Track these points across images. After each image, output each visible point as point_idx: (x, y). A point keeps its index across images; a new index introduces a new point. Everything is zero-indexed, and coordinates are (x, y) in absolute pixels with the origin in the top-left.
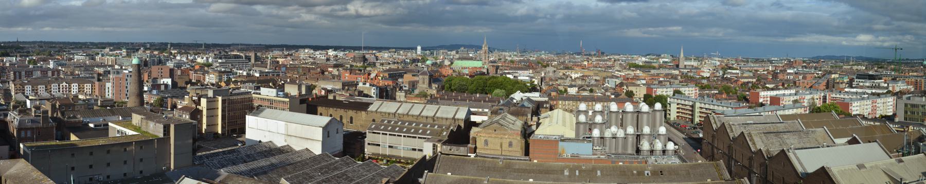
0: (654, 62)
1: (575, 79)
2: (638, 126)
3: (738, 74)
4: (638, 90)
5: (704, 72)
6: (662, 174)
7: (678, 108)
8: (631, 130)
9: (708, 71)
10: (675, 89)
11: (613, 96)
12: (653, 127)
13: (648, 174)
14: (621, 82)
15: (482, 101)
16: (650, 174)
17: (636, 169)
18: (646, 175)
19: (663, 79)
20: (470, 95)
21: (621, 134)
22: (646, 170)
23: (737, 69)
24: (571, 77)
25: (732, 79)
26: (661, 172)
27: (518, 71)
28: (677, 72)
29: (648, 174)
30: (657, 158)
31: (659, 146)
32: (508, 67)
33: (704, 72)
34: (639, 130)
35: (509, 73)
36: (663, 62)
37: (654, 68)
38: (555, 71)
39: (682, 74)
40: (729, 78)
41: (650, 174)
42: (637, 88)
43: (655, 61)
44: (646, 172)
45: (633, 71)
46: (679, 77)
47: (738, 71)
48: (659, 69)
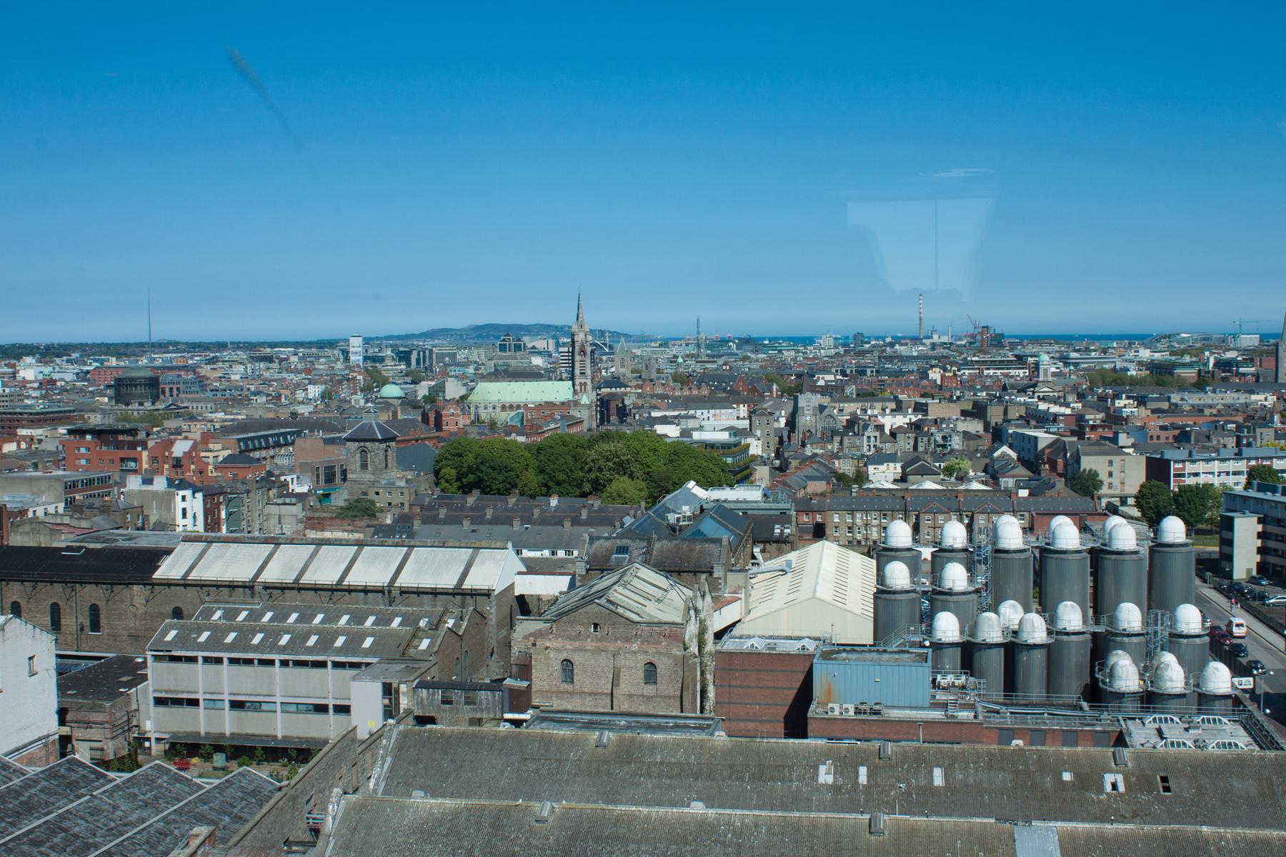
0: (1184, 365)
1: (893, 434)
2: (1099, 606)
4: (1115, 469)
6: (1167, 789)
8: (1072, 616)
10: (1253, 463)
11: (1024, 493)
13: (1114, 786)
14: (1057, 440)
15: (567, 524)
16: (1122, 788)
17: (1073, 765)
18: (1109, 788)
20: (526, 501)
21: (1036, 630)
22: (1111, 772)
24: (880, 428)
26: (1164, 779)
27: (699, 412)
29: (1114, 786)
30: (1164, 726)
31: (1174, 676)
32: (663, 397)
35: (665, 420)
36: (1218, 364)
38: (822, 408)
41: (1122, 788)
42: (1111, 463)
43: (1187, 359)
44: (1109, 778)
46: (1277, 418)
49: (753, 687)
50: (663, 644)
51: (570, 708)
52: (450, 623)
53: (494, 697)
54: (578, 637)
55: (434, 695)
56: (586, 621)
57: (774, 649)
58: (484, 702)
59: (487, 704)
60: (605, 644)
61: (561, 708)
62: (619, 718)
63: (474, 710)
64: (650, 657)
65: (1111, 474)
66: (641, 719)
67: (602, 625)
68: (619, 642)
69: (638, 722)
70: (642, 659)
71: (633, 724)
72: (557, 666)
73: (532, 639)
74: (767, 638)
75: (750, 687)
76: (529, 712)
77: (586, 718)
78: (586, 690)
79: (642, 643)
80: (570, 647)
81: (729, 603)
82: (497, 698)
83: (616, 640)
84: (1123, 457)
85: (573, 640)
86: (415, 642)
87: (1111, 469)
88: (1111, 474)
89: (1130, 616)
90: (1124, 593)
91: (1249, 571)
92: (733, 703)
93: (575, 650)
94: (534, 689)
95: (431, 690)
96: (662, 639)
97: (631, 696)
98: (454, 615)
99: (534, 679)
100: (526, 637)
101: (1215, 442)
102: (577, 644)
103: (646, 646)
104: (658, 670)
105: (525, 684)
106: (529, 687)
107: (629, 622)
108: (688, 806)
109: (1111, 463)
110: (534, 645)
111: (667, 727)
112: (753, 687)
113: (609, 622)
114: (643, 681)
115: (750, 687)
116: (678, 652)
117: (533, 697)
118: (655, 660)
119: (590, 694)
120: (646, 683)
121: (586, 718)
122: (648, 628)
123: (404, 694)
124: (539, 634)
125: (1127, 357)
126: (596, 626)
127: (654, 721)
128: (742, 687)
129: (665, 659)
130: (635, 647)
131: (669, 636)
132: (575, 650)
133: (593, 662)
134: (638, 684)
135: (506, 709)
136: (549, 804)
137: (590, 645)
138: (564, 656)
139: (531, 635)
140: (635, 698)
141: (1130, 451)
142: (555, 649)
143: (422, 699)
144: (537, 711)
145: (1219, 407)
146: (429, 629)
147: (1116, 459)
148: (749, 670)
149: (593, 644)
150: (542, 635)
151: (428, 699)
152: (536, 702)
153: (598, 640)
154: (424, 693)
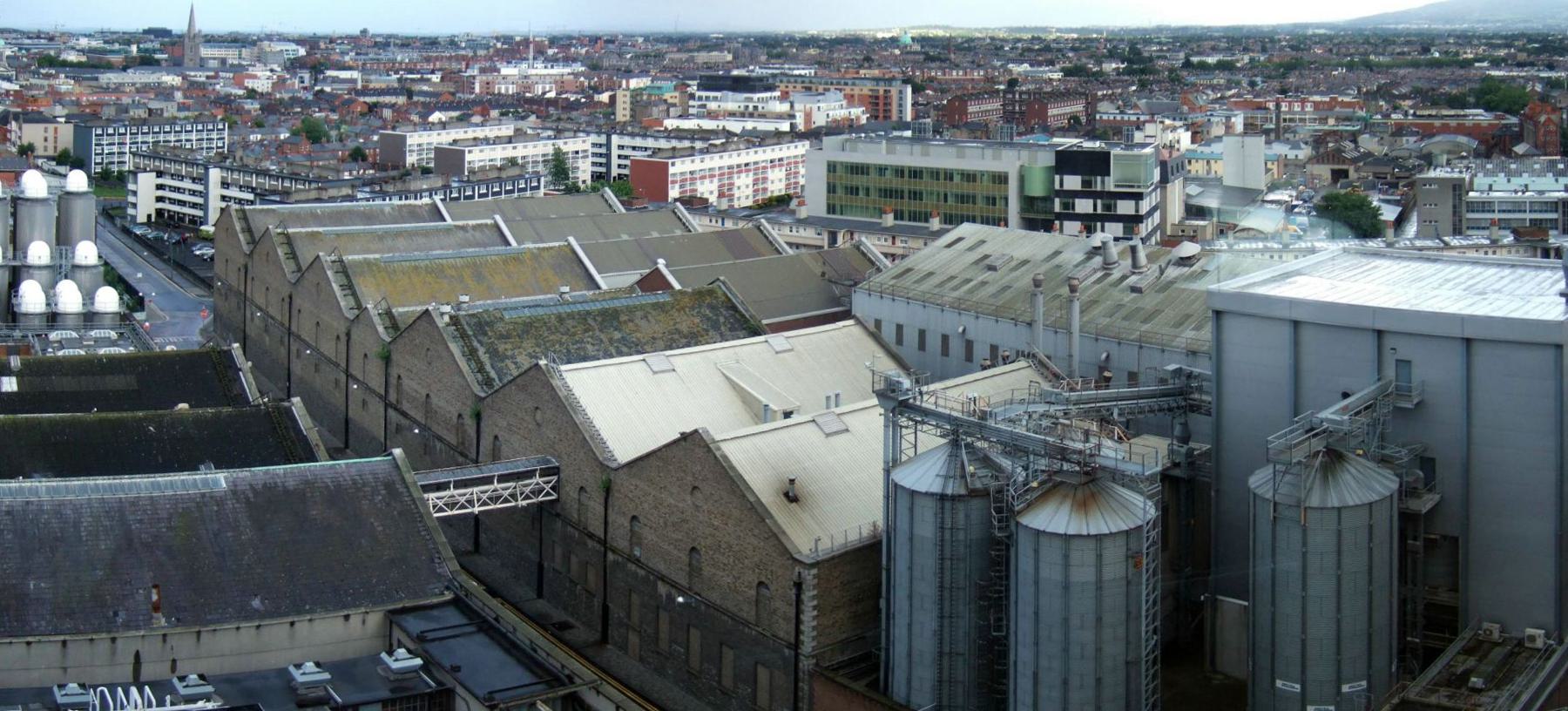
3: (354, 81)
5: (255, 77)
7: (160, 187)
9: (268, 73)
12: (63, 239)
19: (129, 101)
23: (350, 68)
25: (338, 96)
28: (175, 80)
33: (255, 77)
34: (19, 253)
37: (110, 67)
39: (191, 87)
40: (329, 94)
42: (46, 130)
43: (117, 46)
45: (48, 76)
47: (355, 74)
48: (125, 69)
65: (46, 140)
84: (56, 125)
87: (46, 135)
88: (46, 140)
89: (39, 252)
90: (36, 234)
91: (149, 216)
101: (132, 113)
109: (46, 130)
125: (70, 44)
141: (63, 120)
145: (138, 86)
147: (51, 127)
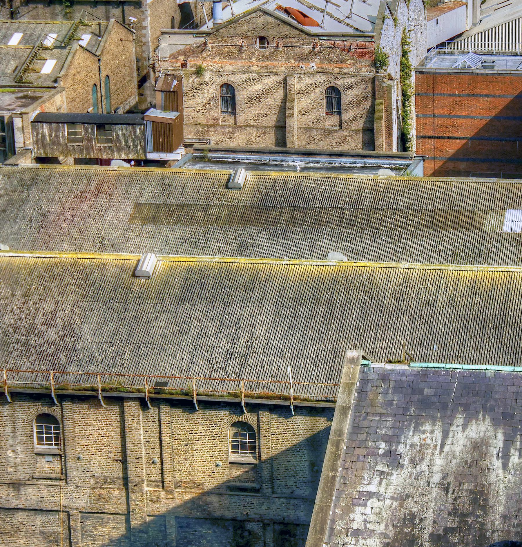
49: (465, 117)
50: (348, 62)
51: (232, 145)
52: (86, 39)
53: (135, 133)
54: (239, 54)
55: (57, 130)
56: (249, 34)
57: (492, 67)
58: (122, 139)
59: (126, 141)
60: (275, 63)
61: (220, 146)
62: (294, 157)
63: (110, 148)
64: (332, 80)
66: (322, 159)
67: (270, 40)
68: (292, 61)
69: (318, 162)
70: (323, 81)
71: (311, 165)
72: (216, 92)
73: (181, 58)
74: (485, 54)
75: (460, 117)
76: (179, 151)
77: (253, 158)
78: (252, 123)
79: (322, 60)
80: (231, 68)
81: (450, 9)
82: (138, 133)
83: (288, 58)
85: (234, 58)
86: (37, 64)
92: (438, 138)
93: (237, 72)
94: (186, 122)
95: (54, 125)
96: (348, 57)
97: (309, 129)
98: (90, 29)
99: (185, 110)
100: (173, 56)
102: (239, 63)
103: (327, 66)
104: (343, 96)
105: (171, 115)
106: (181, 117)
107: (304, 36)
108: (324, 257)
110: (184, 65)
111: (353, 168)
112: (465, 117)
113: (278, 35)
114: (324, 111)
115: (460, 117)
116: (366, 72)
117: (185, 132)
118: (340, 83)
119: (257, 127)
120: (327, 114)
121: (253, 158)
122: (328, 43)
123: (18, 129)
124: (190, 52)
126: (262, 39)
127: (338, 161)
128: (449, 117)
129: (351, 82)
130: (314, 65)
131: (356, 51)
132: (237, 72)
133: (259, 86)
134: (318, 114)
135: (150, 145)
136: (153, 255)
137: (256, 64)
138: (220, 80)
139: (179, 53)
140: (315, 131)
142: (212, 70)
143: (43, 136)
144: (191, 150)
146: (56, 47)
148: (459, 95)
149: (260, 64)
150: (193, 53)
151: (50, 136)
152: (189, 137)
153: (266, 58)
154: (45, 129)
